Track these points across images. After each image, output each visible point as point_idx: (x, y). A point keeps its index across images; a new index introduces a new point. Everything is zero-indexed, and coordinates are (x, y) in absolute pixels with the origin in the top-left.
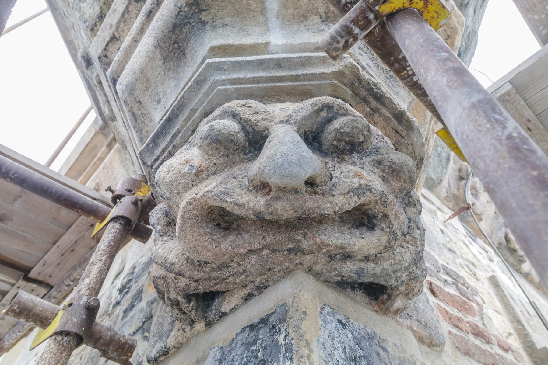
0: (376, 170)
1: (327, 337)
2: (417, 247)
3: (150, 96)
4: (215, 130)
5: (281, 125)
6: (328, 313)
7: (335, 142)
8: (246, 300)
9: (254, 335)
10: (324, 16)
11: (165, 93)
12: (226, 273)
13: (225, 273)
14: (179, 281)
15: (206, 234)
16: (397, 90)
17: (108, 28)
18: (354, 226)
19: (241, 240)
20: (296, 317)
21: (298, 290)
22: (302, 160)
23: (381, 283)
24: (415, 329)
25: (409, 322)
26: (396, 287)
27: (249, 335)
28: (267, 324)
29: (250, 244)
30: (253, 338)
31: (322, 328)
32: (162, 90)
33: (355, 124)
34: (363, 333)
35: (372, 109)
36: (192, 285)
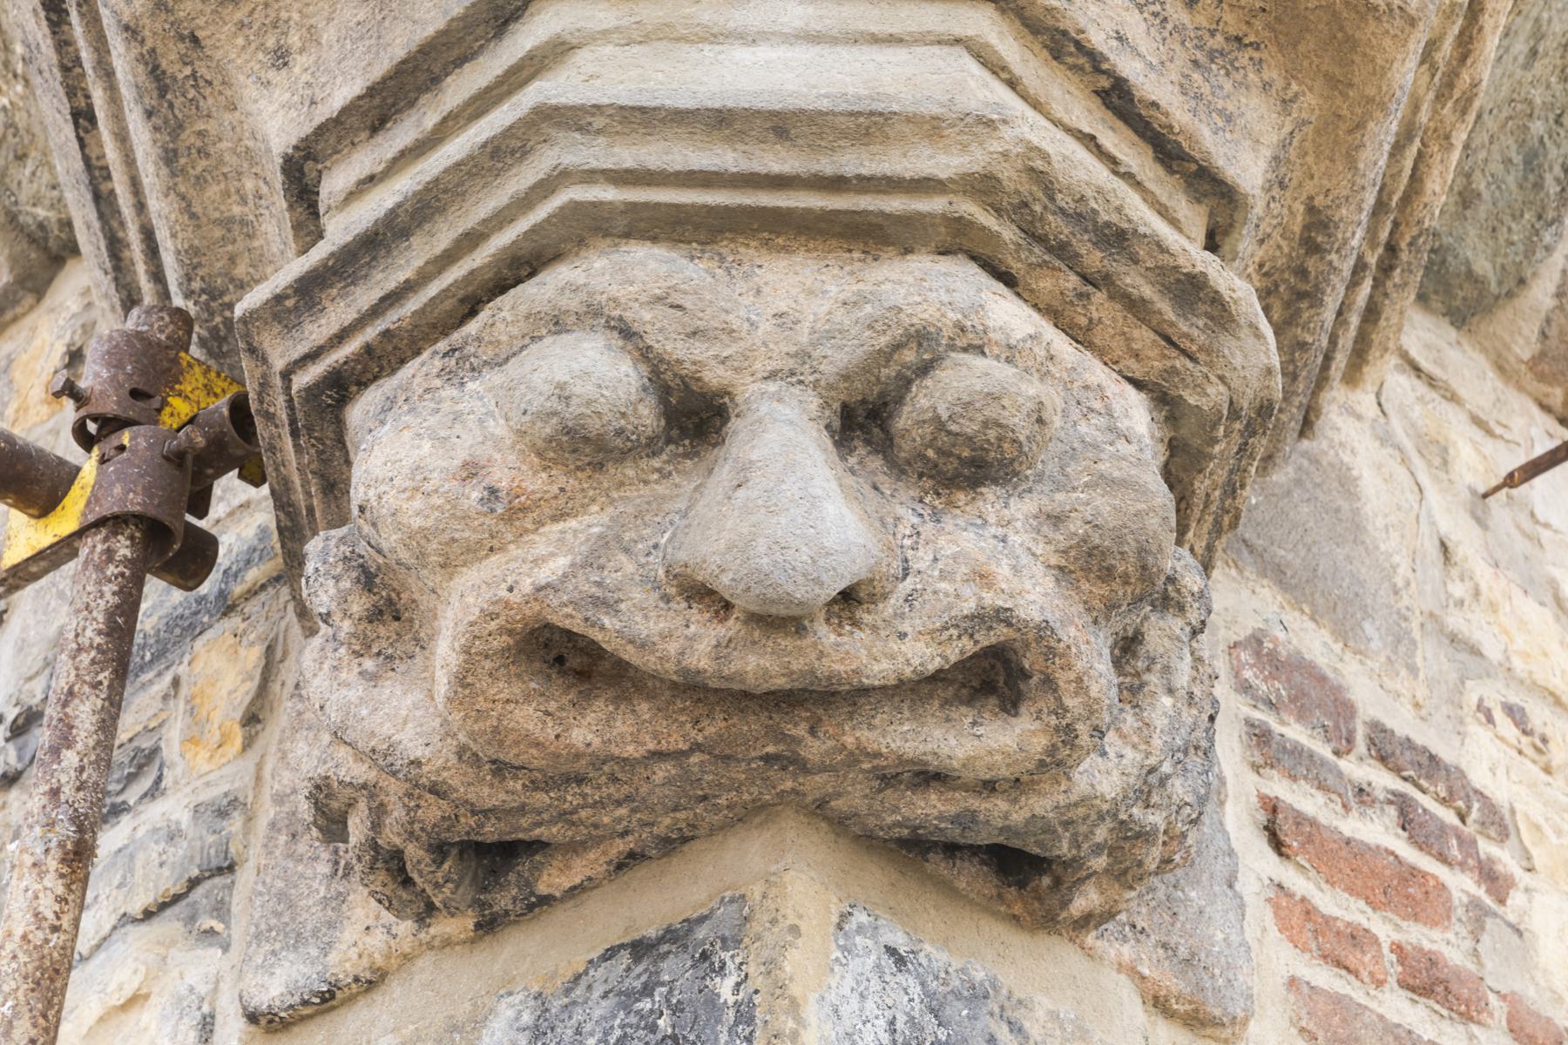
0: (1041, 546)
1: (847, 991)
2: (1148, 755)
3: (241, 25)
4: (575, 401)
5: (772, 387)
6: (860, 929)
7: (930, 453)
8: (620, 867)
9: (646, 970)
11: (312, 36)
12: (572, 798)
13: (569, 798)
14: (422, 803)
15: (528, 698)
16: (1231, 108)
18: (964, 691)
19: (631, 719)
20: (769, 938)
21: (781, 866)
22: (821, 562)
23: (1027, 849)
24: (1146, 972)
25: (1127, 952)
26: (1074, 859)
27: (628, 969)
28: (685, 947)
29: (656, 736)
30: (644, 978)
31: (837, 968)
32: (296, 16)
33: (991, 412)
34: (958, 983)
35: (1086, 279)
36: (463, 820)
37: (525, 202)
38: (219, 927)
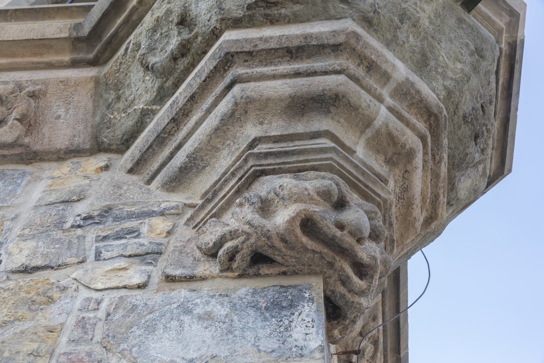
8: (279, 274)
10: (388, 159)
11: (270, 123)
17: (252, 44)
37: (321, 160)
38: (153, 262)
